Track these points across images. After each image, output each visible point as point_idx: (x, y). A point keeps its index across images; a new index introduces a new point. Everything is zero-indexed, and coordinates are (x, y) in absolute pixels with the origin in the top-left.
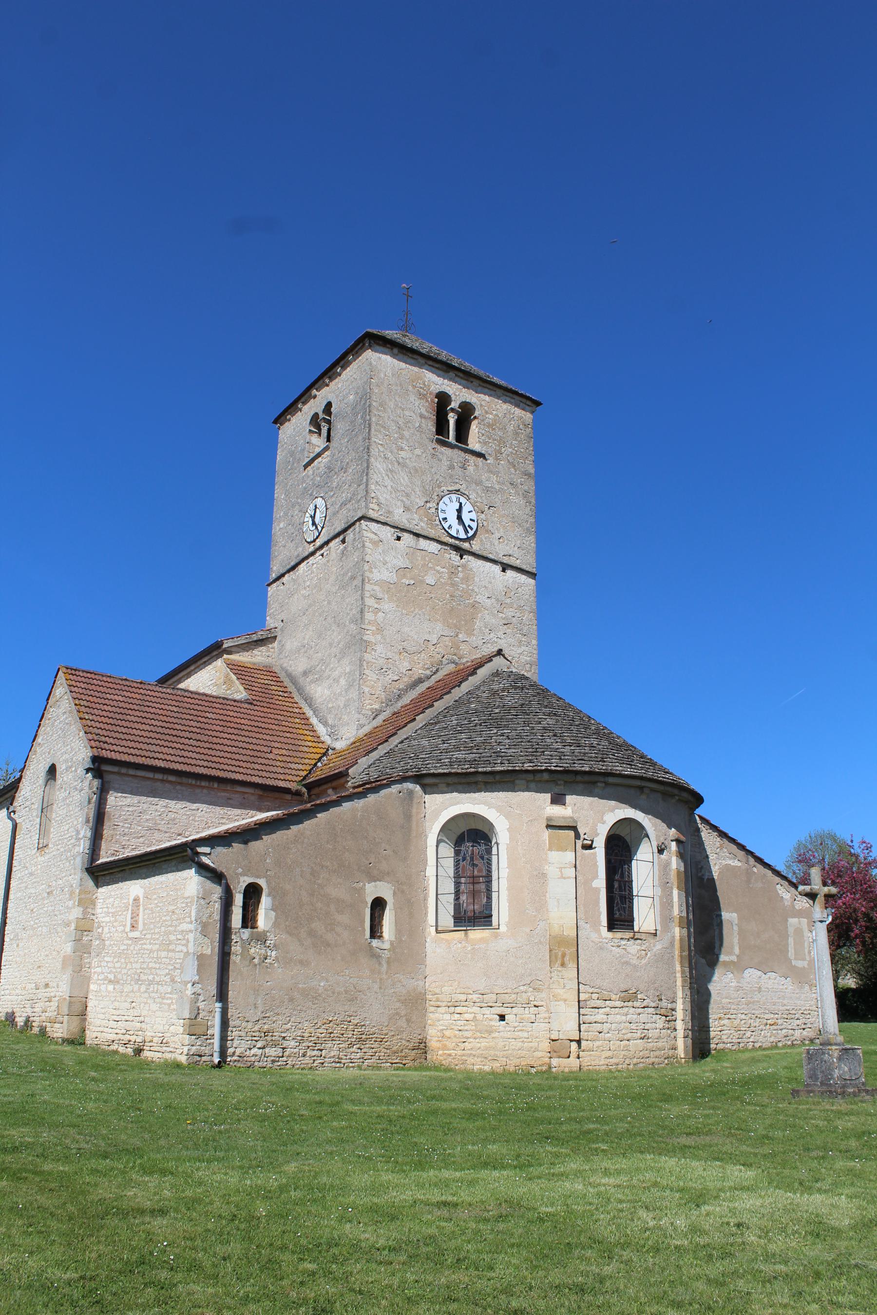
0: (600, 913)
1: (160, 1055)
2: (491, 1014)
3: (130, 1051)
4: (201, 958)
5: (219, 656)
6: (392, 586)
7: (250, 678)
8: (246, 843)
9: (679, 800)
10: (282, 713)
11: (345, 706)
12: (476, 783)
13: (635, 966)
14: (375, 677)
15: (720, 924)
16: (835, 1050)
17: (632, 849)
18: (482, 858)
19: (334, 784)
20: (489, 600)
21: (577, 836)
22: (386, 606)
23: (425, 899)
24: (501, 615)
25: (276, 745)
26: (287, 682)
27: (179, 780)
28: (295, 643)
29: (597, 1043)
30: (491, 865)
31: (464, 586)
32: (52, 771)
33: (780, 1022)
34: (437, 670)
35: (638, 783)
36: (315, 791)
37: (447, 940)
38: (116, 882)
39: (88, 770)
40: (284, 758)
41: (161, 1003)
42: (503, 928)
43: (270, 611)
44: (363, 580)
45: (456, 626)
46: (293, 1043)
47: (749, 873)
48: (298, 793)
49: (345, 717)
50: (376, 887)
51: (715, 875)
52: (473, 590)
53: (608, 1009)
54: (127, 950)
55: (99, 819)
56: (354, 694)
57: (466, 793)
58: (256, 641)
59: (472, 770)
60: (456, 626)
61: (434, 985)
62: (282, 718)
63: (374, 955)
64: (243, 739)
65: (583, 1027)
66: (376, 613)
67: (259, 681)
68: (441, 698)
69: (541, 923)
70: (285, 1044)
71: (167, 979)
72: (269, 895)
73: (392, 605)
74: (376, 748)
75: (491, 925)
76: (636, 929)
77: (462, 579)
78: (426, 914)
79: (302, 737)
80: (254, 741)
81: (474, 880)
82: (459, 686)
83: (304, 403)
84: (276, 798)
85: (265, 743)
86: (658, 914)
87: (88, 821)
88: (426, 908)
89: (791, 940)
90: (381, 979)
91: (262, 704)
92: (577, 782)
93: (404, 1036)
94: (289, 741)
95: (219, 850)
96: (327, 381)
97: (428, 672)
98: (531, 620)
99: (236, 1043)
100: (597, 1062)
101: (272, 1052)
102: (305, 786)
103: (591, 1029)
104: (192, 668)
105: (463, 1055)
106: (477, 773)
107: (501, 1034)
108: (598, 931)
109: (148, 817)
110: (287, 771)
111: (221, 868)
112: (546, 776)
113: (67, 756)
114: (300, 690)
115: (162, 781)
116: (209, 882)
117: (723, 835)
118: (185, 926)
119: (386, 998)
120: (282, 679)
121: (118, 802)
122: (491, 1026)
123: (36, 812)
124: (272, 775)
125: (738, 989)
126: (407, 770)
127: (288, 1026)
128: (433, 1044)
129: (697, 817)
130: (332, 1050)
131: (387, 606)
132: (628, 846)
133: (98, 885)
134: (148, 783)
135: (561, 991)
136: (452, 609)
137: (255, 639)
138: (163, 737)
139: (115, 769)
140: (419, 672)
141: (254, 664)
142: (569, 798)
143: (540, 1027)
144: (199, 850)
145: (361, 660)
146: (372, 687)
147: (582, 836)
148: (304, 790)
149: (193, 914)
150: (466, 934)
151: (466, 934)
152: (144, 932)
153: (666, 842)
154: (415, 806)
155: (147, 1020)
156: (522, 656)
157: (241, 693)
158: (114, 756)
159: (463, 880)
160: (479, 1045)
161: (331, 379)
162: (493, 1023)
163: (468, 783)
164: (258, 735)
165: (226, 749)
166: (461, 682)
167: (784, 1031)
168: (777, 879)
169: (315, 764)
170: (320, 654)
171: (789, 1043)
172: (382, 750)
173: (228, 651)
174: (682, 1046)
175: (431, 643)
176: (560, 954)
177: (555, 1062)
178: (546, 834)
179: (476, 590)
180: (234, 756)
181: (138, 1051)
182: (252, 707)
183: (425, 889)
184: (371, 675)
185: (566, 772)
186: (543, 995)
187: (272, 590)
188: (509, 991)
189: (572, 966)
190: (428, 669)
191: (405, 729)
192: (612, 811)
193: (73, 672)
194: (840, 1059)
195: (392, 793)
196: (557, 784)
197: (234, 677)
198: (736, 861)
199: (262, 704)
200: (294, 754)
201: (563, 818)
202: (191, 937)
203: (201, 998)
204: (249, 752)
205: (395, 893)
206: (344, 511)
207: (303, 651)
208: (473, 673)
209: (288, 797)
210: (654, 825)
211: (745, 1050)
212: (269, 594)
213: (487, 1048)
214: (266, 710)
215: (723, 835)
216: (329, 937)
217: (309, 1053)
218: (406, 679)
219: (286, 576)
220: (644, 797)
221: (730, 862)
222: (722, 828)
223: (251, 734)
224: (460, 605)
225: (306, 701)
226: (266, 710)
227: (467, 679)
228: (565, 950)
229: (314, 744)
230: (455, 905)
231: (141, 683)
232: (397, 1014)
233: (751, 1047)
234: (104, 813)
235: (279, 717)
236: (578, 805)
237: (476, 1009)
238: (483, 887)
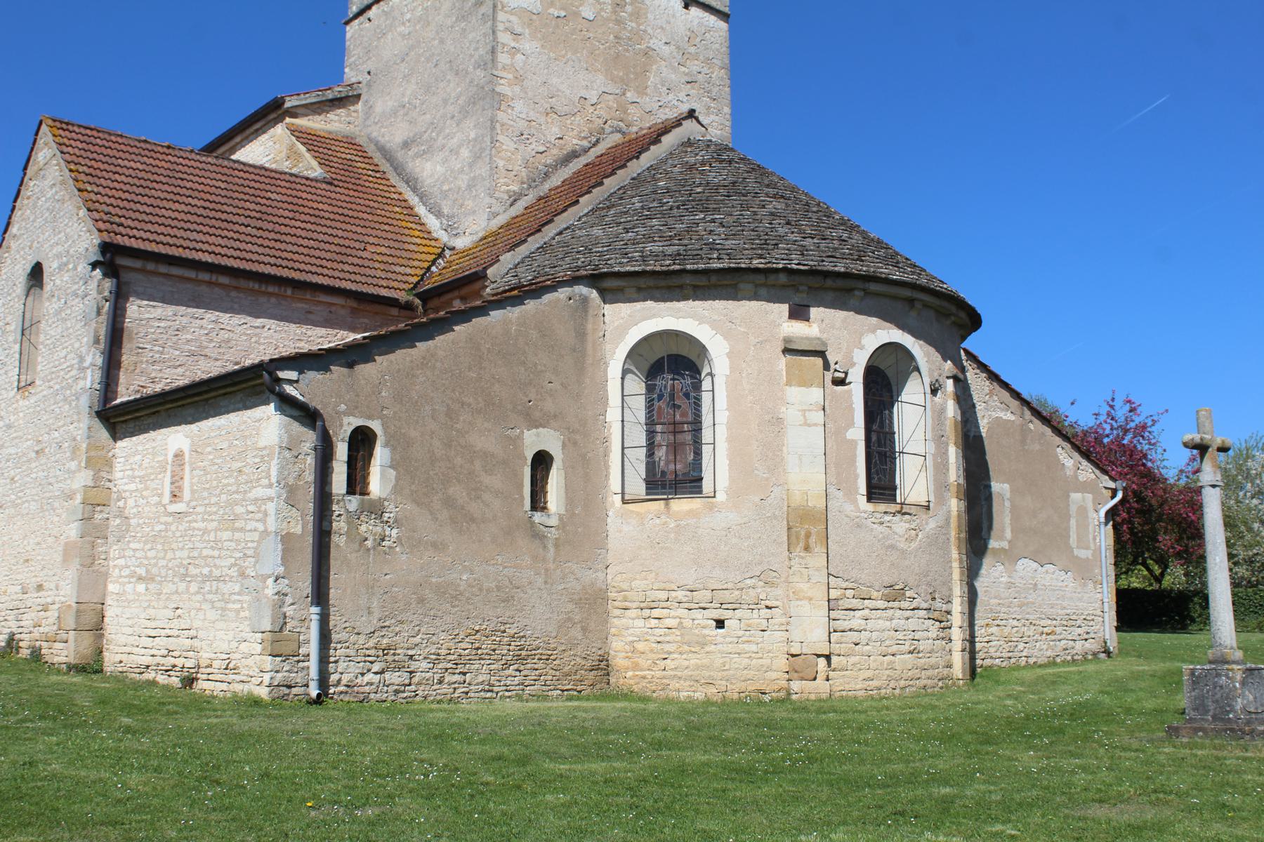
0: (857, 476)
1: (224, 686)
2: (704, 620)
3: (175, 681)
4: (287, 540)
5: (279, 119)
6: (535, 17)
7: (325, 151)
8: (351, 365)
9: (954, 323)
10: (375, 198)
11: (469, 187)
12: (681, 287)
13: (903, 552)
14: (512, 146)
15: (989, 498)
16: (1237, 672)
17: (894, 388)
18: (687, 395)
19: (464, 291)
20: (667, 47)
21: (826, 366)
22: (527, 46)
23: (606, 455)
24: (683, 69)
25: (371, 240)
26: (378, 158)
27: (234, 282)
28: (390, 103)
29: (853, 660)
30: (700, 406)
31: (634, 25)
32: (36, 274)
33: (1058, 630)
34: (598, 141)
35: (907, 293)
36: (435, 302)
37: (638, 514)
38: (146, 431)
39: (94, 265)
40: (385, 259)
41: (223, 609)
42: (721, 496)
43: (349, 60)
44: (495, 6)
45: (622, 80)
46: (424, 665)
47: (1024, 431)
48: (408, 307)
49: (470, 204)
50: (538, 435)
51: (984, 432)
52: (645, 31)
53: (867, 612)
54: (166, 530)
55: (115, 339)
56: (482, 170)
57: (665, 300)
58: (331, 101)
59: (677, 267)
60: (622, 80)
61: (619, 578)
62: (376, 205)
63: (536, 534)
64: (324, 230)
65: (834, 636)
66: (513, 55)
67: (339, 155)
68: (613, 173)
69: (776, 489)
70: (414, 665)
71: (233, 572)
72: (386, 445)
73: (535, 44)
74: (525, 241)
75: (701, 492)
76: (898, 500)
77: (631, 15)
78: (607, 476)
79: (407, 231)
80: (340, 233)
81: (675, 428)
82: (638, 158)
84: (377, 313)
85: (356, 237)
86: (931, 479)
87: (97, 341)
88: (607, 467)
89: (1073, 522)
90: (547, 570)
91: (346, 185)
92: (826, 289)
93: (579, 650)
94: (390, 236)
95: (311, 375)
97: (585, 143)
98: (722, 79)
99: (342, 666)
100: (852, 686)
101: (394, 678)
102: (418, 295)
103: (844, 640)
104: (238, 139)
105: (664, 677)
106: (684, 271)
107: (720, 647)
108: (855, 502)
109: (189, 337)
110: (390, 275)
111: (315, 404)
112: (783, 278)
113: (60, 248)
114: (398, 169)
115: (210, 283)
116: (296, 424)
117: (994, 377)
118: (260, 492)
119: (554, 596)
120: (370, 155)
121: (142, 313)
122: (705, 636)
123: (13, 335)
124: (370, 280)
125: (1010, 585)
126: (578, 268)
127: (417, 640)
128: (619, 661)
129: (962, 352)
130: (480, 674)
131: (528, 45)
132: (889, 384)
133: (115, 437)
134: (189, 286)
135: (804, 586)
136: (618, 56)
137: (330, 97)
138: (207, 221)
139: (138, 264)
140: (573, 142)
141: (330, 133)
142: (815, 312)
143: (775, 638)
144: (281, 374)
145: (493, 121)
146: (509, 160)
147: (833, 367)
148: (417, 301)
149: (274, 473)
150: (667, 504)
151: (667, 504)
152: (193, 503)
153: (941, 380)
154: (590, 319)
155: (201, 634)
156: (717, 124)
157: (312, 168)
158: (134, 244)
159: (659, 428)
160: (686, 663)
162: (706, 632)
163: (669, 288)
164: (344, 226)
165: (300, 241)
166: (640, 153)
167: (1063, 642)
168: (1058, 440)
169: (429, 269)
170: (428, 116)
171: (1069, 658)
172: (534, 243)
173: (293, 113)
174: (958, 661)
175: (588, 103)
176: (803, 533)
177: (796, 686)
178: (783, 362)
179: (650, 31)
180: (312, 252)
181: (189, 681)
182: (332, 188)
183: (606, 440)
184: (507, 143)
185: (813, 272)
186: (779, 592)
187: (351, 30)
188: (730, 586)
189: (819, 549)
190: (585, 138)
191: (565, 214)
192: (873, 330)
193: (64, 126)
194: (1243, 683)
195: (558, 300)
196: (797, 291)
197: (302, 149)
198: (1009, 414)
199: (346, 185)
200: (398, 253)
201: (807, 338)
202: (271, 507)
203: (289, 600)
204: (333, 248)
205: (564, 446)
207: (401, 113)
208: (656, 141)
209: (395, 311)
210: (927, 355)
211: (1018, 668)
212: (348, 35)
213: (698, 667)
214: (351, 193)
215: (994, 377)
216: (474, 508)
217: (448, 678)
218: (555, 151)
219: (374, 8)
220: (913, 313)
221: (1002, 415)
222: (993, 368)
223: (333, 224)
224: (627, 50)
225: (407, 183)
226: (351, 193)
227: (648, 149)
228: (806, 528)
229: (424, 242)
230: (647, 463)
231: (169, 147)
232: (569, 619)
233: (1023, 663)
234: (122, 330)
235: (372, 204)
236: (826, 321)
237: (682, 612)
238: (688, 437)
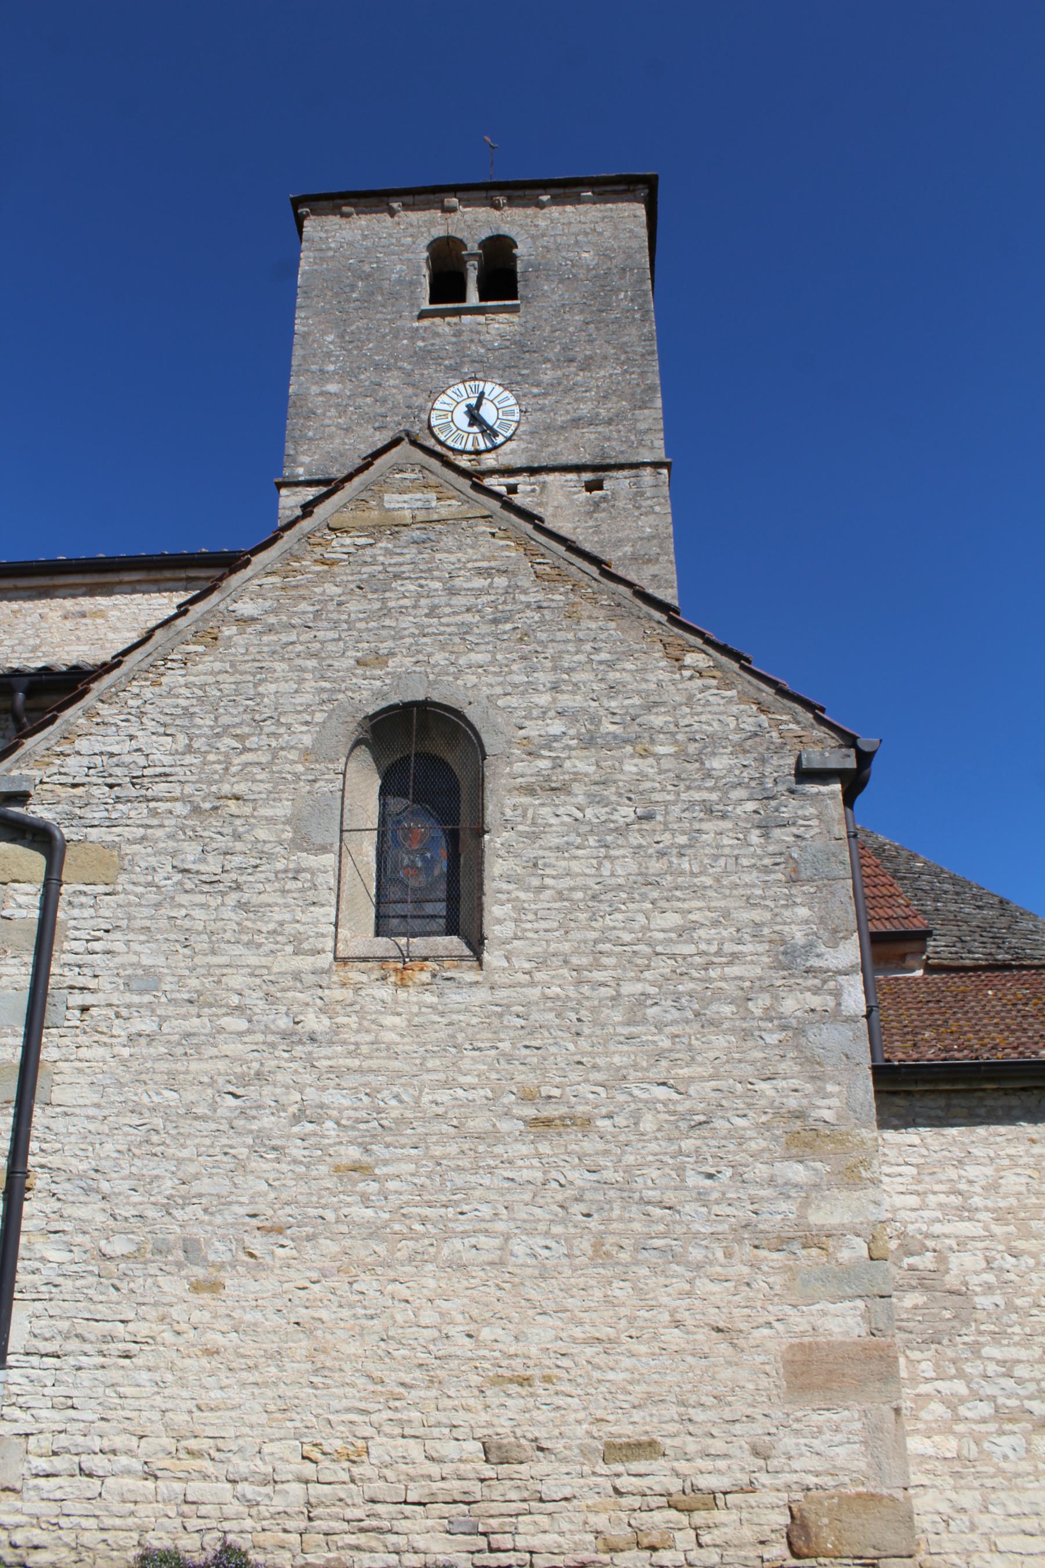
83: (406, 207)
96: (502, 200)
161: (511, 202)
206: (589, 434)
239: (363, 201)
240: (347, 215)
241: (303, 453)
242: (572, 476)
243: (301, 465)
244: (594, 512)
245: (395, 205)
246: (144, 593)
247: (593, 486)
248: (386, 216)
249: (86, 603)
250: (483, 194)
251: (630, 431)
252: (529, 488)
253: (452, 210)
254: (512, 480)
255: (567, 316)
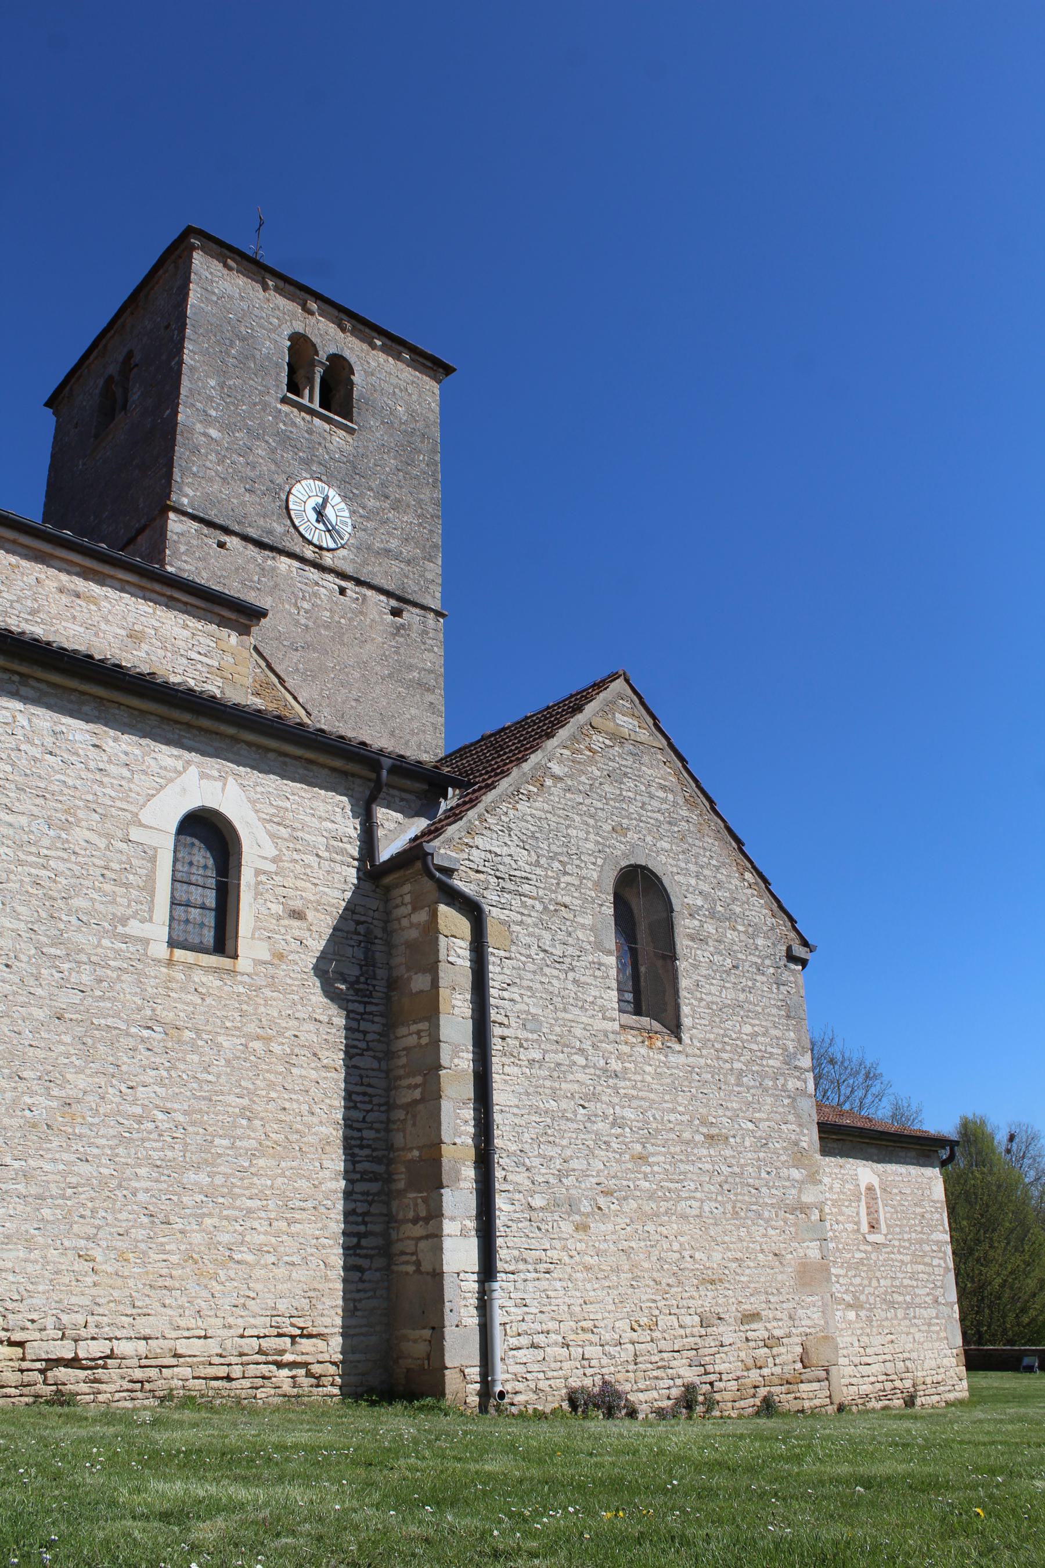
41: (928, 1332)
54: (867, 1258)
83: (277, 289)
96: (349, 326)
133: (825, 1152)
152: (890, 1237)
206: (396, 567)
239: (245, 263)
240: (230, 269)
241: (189, 485)
242: (383, 598)
243: (186, 496)
244: (396, 634)
245: (270, 283)
246: (132, 595)
247: (396, 613)
248: (258, 287)
249: (80, 584)
250: (336, 313)
251: (420, 576)
252: (355, 596)
253: (311, 313)
254: (343, 584)
255: (385, 456)
